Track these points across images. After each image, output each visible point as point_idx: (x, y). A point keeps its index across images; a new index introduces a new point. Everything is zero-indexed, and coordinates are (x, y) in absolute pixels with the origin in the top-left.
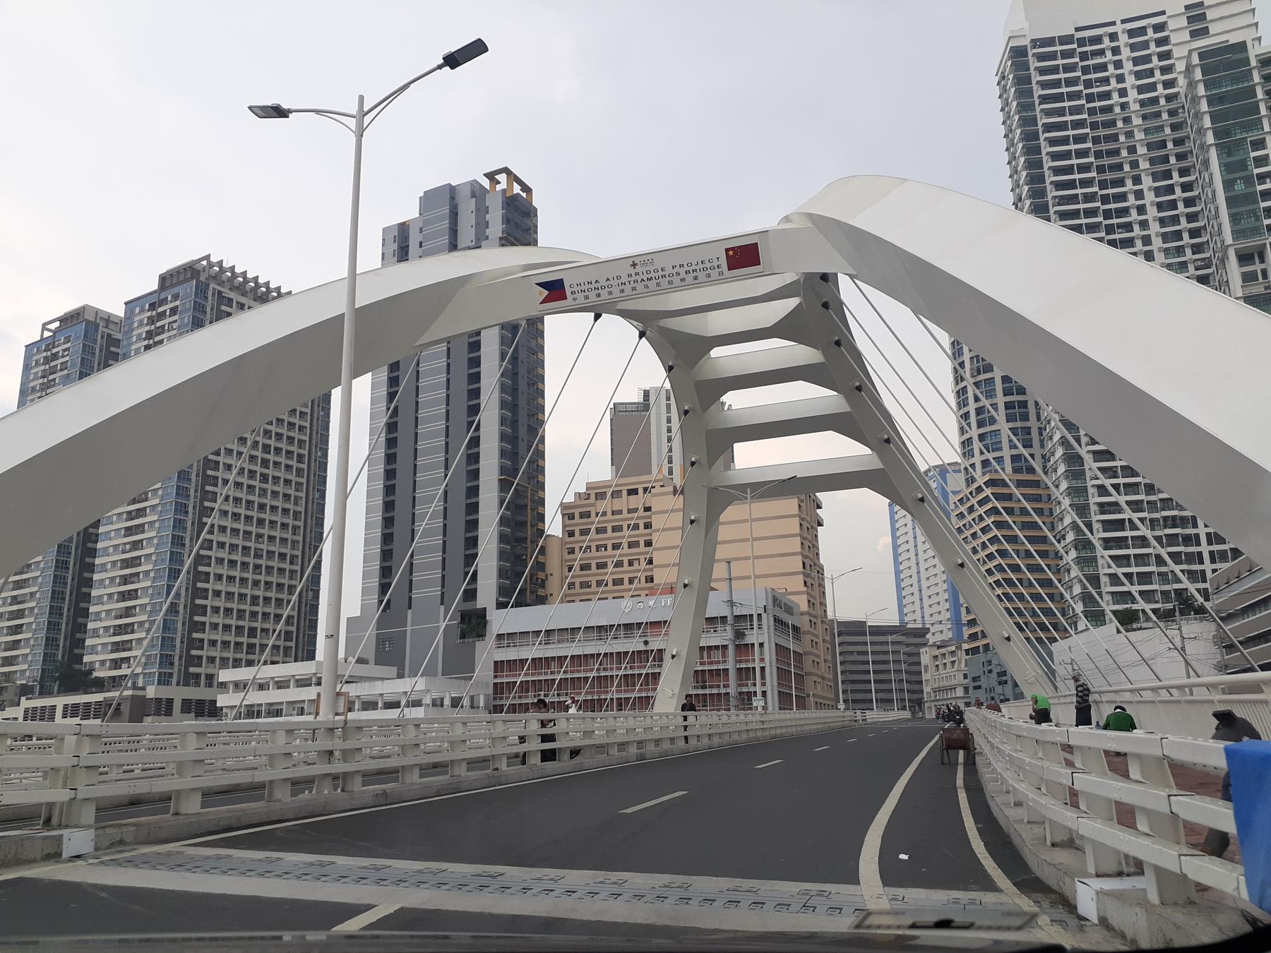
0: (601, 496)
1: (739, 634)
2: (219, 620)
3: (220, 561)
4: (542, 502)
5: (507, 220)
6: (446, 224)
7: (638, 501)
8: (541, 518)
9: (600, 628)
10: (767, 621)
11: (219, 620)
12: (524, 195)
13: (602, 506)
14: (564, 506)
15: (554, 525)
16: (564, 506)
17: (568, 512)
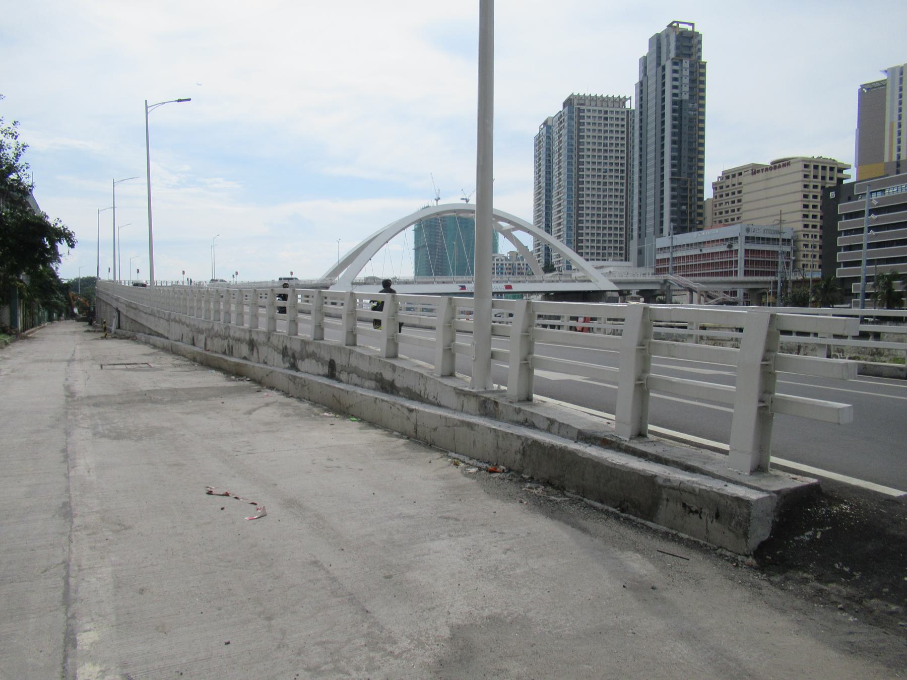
0: (728, 177)
1: (730, 246)
2: (589, 244)
3: (588, 221)
4: (702, 184)
5: (677, 48)
6: (655, 55)
7: (735, 181)
8: (702, 191)
9: (688, 245)
10: (741, 240)
11: (589, 244)
12: (690, 28)
13: (729, 182)
14: (714, 184)
15: (708, 193)
16: (714, 184)
17: (715, 186)
